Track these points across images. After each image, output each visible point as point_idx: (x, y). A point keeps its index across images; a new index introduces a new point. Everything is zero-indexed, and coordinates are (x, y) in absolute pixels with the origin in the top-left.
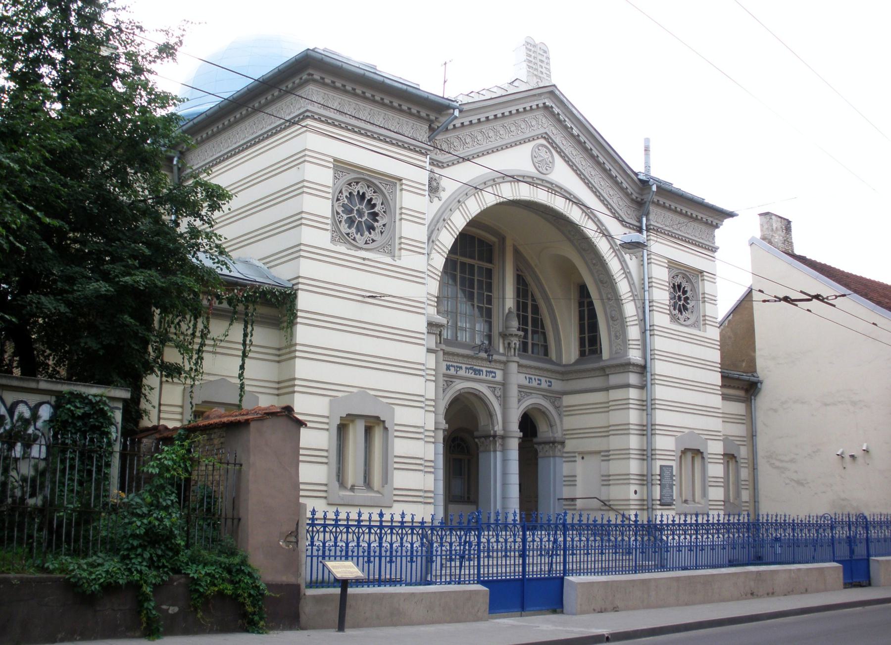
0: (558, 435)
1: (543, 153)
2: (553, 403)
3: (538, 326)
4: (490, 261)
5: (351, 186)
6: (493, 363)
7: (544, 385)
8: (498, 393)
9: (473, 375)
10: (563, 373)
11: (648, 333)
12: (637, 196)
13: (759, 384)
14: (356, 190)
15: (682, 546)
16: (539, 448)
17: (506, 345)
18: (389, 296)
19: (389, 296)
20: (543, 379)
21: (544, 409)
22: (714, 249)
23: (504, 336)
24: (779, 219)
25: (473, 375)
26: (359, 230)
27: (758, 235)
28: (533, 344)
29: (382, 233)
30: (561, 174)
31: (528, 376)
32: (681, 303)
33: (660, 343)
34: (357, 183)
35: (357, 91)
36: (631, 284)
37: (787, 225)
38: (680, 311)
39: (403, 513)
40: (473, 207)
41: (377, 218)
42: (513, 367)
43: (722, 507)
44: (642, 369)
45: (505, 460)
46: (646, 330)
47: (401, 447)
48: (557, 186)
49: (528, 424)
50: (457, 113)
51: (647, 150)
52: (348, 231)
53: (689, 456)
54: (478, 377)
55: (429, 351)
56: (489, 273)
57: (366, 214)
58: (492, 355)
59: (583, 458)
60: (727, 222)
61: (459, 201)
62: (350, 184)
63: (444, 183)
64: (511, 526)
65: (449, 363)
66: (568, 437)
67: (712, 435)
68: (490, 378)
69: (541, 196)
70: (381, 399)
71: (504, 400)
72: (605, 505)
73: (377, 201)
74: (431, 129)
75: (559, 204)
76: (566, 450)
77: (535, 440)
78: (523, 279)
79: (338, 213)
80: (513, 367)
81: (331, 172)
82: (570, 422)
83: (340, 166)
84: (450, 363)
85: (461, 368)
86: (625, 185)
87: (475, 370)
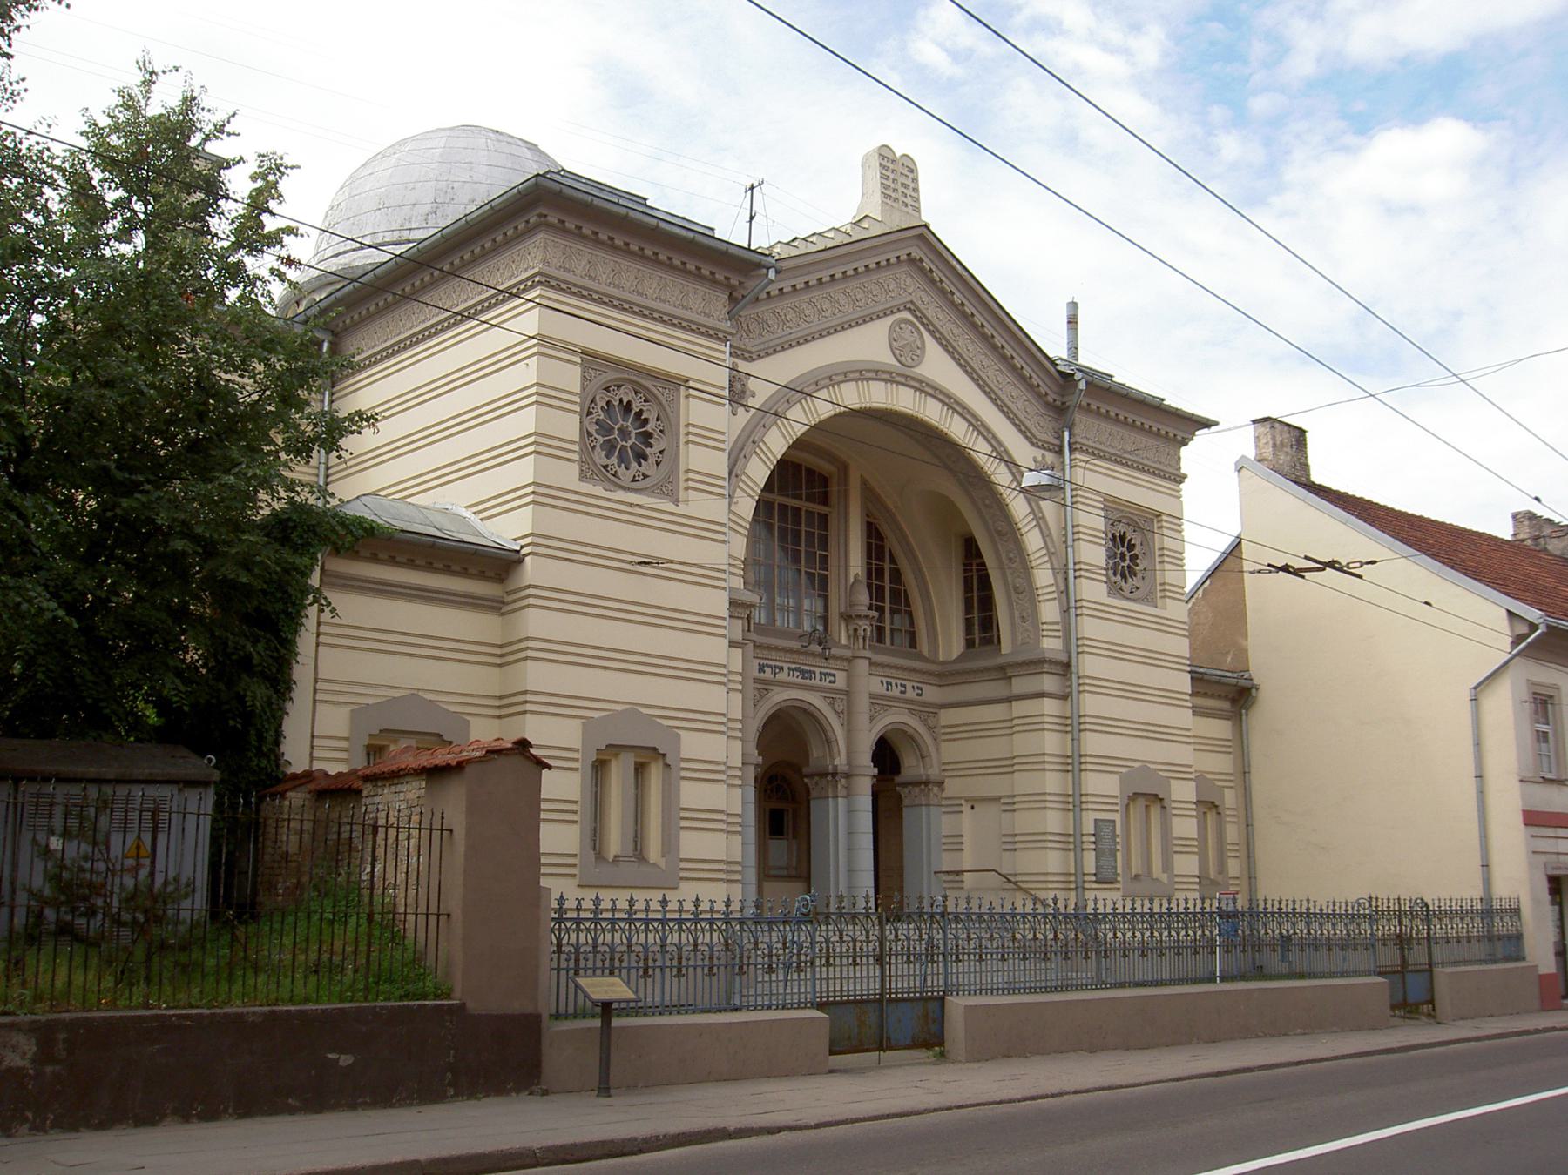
0: (934, 772)
1: (907, 333)
2: (924, 722)
3: (900, 600)
4: (825, 501)
5: (609, 392)
6: (830, 661)
7: (911, 694)
8: (840, 706)
9: (800, 680)
10: (940, 675)
11: (1072, 611)
12: (1055, 396)
13: (1254, 691)
14: (617, 398)
16: (904, 792)
17: (851, 632)
18: (672, 562)
19: (672, 562)
20: (909, 685)
21: (910, 731)
22: (1180, 479)
23: (847, 618)
24: (1286, 428)
25: (800, 680)
26: (622, 459)
27: (1251, 453)
28: (892, 630)
29: (658, 464)
30: (937, 366)
31: (885, 680)
32: (1126, 564)
33: (1089, 628)
34: (619, 387)
35: (616, 241)
36: (1046, 536)
37: (1299, 436)
38: (1123, 576)
39: (697, 899)
40: (800, 419)
41: (651, 441)
42: (862, 667)
43: (1196, 887)
44: (1065, 668)
45: (851, 812)
46: (1069, 608)
47: (692, 794)
48: (928, 385)
49: (886, 755)
50: (772, 274)
51: (1072, 321)
52: (605, 461)
53: (1141, 802)
55: (732, 644)
56: (824, 519)
57: (633, 435)
58: (829, 649)
59: (973, 808)
60: (1201, 434)
62: (607, 389)
63: (752, 384)
64: (861, 917)
65: (762, 662)
66: (946, 774)
67: (1181, 771)
68: (826, 684)
69: (904, 401)
70: (658, 720)
71: (848, 716)
72: (1009, 881)
73: (650, 414)
74: (732, 299)
75: (932, 412)
76: (944, 795)
77: (898, 779)
78: (876, 529)
79: (590, 434)
80: (862, 667)
81: (578, 370)
83: (591, 360)
84: (766, 662)
86: (1036, 381)
87: (803, 672)
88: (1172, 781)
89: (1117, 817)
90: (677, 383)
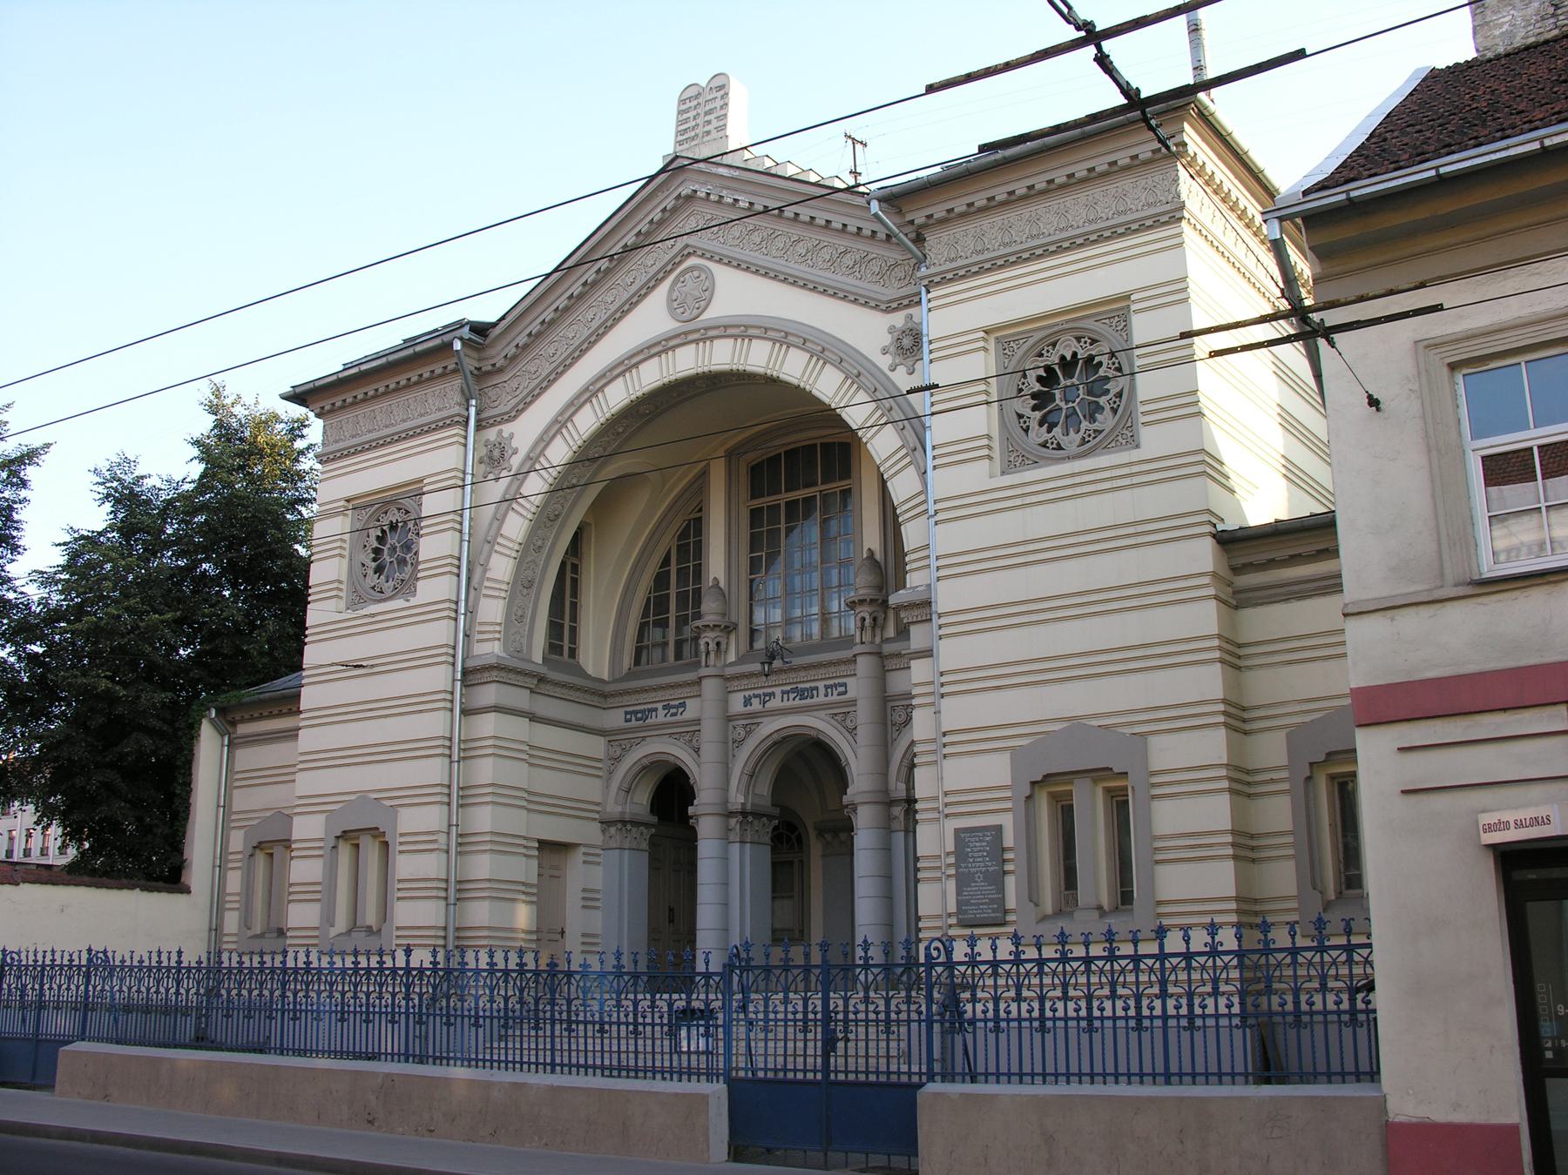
6: (773, 678)
9: (798, 702)
15: (325, 1012)
25: (798, 702)
42: (864, 665)
47: (406, 866)
54: (809, 701)
65: (747, 693)
68: (835, 698)
69: (686, 362)
75: (722, 356)
82: (590, 789)
84: (751, 693)
85: (773, 694)
87: (803, 690)
88: (1152, 740)
89: (1006, 821)
90: (416, 489)
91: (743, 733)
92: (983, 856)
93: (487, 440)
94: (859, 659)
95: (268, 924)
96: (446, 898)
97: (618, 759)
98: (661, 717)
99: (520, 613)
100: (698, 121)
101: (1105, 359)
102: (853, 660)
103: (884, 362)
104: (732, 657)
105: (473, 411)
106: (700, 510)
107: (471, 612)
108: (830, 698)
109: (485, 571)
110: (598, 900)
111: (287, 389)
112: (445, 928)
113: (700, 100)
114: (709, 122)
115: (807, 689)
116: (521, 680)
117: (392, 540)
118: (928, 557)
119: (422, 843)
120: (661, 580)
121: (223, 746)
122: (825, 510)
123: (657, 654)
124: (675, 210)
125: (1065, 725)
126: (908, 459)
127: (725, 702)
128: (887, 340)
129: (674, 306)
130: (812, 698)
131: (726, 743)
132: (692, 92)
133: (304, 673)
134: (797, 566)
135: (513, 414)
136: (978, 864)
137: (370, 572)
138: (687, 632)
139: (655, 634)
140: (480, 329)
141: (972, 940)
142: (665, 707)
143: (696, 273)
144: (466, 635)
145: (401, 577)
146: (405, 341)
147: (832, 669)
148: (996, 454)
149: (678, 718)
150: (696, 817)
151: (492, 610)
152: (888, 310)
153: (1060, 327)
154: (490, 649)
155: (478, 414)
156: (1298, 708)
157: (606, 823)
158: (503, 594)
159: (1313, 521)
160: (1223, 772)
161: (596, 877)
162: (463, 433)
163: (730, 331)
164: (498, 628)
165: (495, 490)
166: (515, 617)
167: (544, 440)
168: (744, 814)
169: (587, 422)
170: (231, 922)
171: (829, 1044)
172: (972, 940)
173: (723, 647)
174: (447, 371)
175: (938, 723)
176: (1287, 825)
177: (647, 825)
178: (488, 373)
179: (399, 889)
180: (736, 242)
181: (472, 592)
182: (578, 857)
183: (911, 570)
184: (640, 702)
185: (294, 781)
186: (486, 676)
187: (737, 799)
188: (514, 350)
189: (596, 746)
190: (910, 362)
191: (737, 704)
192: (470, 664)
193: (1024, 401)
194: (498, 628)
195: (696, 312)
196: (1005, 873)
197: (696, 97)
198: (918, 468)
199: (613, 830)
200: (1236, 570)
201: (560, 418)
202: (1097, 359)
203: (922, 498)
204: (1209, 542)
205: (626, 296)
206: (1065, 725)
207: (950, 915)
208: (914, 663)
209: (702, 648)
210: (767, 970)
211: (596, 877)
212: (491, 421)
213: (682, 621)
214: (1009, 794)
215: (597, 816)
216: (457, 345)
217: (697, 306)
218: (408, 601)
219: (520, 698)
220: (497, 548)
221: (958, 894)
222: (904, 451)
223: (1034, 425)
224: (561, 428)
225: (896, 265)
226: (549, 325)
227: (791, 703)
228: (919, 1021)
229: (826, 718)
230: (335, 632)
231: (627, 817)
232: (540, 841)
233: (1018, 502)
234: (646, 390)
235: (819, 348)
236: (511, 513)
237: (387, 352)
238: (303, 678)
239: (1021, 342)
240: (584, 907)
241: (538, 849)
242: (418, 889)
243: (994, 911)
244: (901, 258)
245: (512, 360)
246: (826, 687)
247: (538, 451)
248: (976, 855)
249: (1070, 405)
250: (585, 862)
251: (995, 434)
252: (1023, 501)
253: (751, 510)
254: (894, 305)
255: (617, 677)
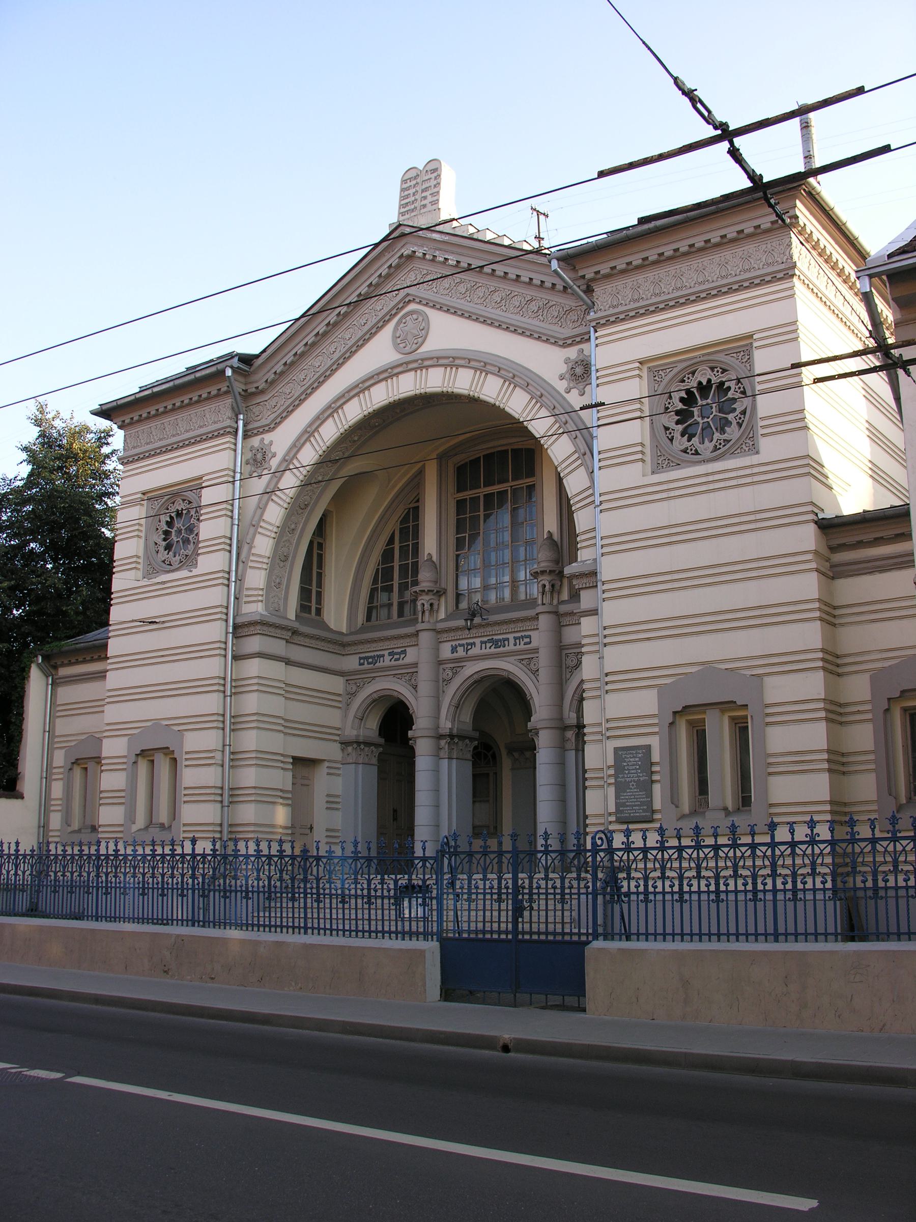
6: (473, 631)
9: (493, 650)
15: (130, 888)
25: (493, 650)
42: (545, 621)
47: (190, 777)
54: (502, 649)
61: (542, 396)
65: (454, 643)
68: (522, 647)
82: (332, 717)
84: (457, 643)
87: (497, 641)
88: (765, 678)
89: (654, 742)
90: (196, 485)
91: (451, 674)
92: (636, 769)
93: (252, 447)
94: (541, 617)
95: (84, 823)
96: (221, 802)
97: (353, 695)
98: (387, 661)
99: (278, 581)
100: (417, 197)
101: (732, 384)
102: (536, 618)
103: (561, 386)
104: (442, 615)
105: (241, 423)
106: (418, 501)
107: (240, 580)
108: (518, 647)
109: (251, 548)
110: (338, 803)
111: (96, 406)
112: (221, 825)
113: (418, 180)
114: (425, 198)
115: (500, 640)
116: (279, 633)
117: (178, 524)
118: (595, 537)
119: (202, 759)
120: (387, 555)
121: (47, 684)
122: (515, 500)
123: (384, 612)
124: (398, 267)
125: (700, 668)
126: (579, 462)
127: (437, 650)
128: (564, 369)
129: (398, 341)
130: (504, 646)
131: (437, 681)
132: (412, 174)
133: (111, 628)
134: (493, 544)
135: (272, 426)
136: (632, 775)
137: (161, 549)
138: (408, 596)
139: (383, 597)
140: (247, 359)
141: (628, 833)
142: (390, 654)
143: (415, 316)
144: (236, 598)
145: (185, 553)
146: (188, 369)
147: (520, 625)
148: (648, 458)
149: (401, 662)
150: (415, 739)
151: (256, 579)
152: (565, 346)
153: (699, 360)
154: (255, 609)
155: (245, 425)
156: (879, 656)
157: (345, 744)
158: (265, 566)
159: (891, 512)
160: (821, 705)
161: (338, 785)
162: (233, 441)
163: (441, 362)
164: (261, 593)
165: (259, 485)
166: (274, 583)
167: (297, 446)
168: (451, 736)
169: (330, 432)
170: (56, 821)
171: (518, 911)
172: (628, 833)
173: (435, 607)
174: (221, 392)
175: (602, 666)
176: (870, 746)
177: (377, 745)
178: (253, 394)
179: (185, 795)
180: (446, 292)
181: (241, 564)
182: (323, 769)
183: (581, 548)
184: (371, 650)
185: (103, 712)
186: (252, 630)
187: (446, 725)
188: (273, 376)
189: (336, 684)
190: (581, 386)
191: (446, 651)
192: (240, 620)
193: (669, 417)
194: (261, 593)
195: (415, 346)
196: (653, 782)
197: (415, 178)
198: (587, 468)
199: (350, 749)
200: (833, 549)
201: (308, 429)
202: (727, 384)
203: (590, 491)
204: (812, 527)
205: (360, 334)
206: (700, 668)
207: (610, 814)
208: (584, 620)
209: (419, 608)
210: (470, 854)
211: (338, 785)
212: (255, 432)
213: (403, 587)
214: (656, 721)
215: (337, 738)
216: (229, 372)
217: (415, 342)
218: (191, 571)
219: (278, 647)
220: (260, 530)
221: (617, 797)
222: (576, 455)
223: (677, 435)
224: (309, 437)
225: (571, 310)
226: (300, 357)
227: (488, 650)
228: (587, 894)
229: (516, 662)
230: (136, 596)
231: (361, 739)
232: (294, 758)
233: (664, 495)
234: (376, 407)
235: (511, 375)
236: (271, 503)
237: (174, 377)
238: (110, 631)
239: (668, 370)
240: (327, 808)
241: (292, 763)
242: (199, 795)
243: (644, 811)
244: (574, 304)
245: (271, 384)
246: (515, 638)
247: (291, 456)
248: (631, 768)
249: (706, 420)
250: (328, 774)
251: (647, 442)
252: (668, 495)
253: (458, 501)
254: (569, 342)
255: (353, 630)
